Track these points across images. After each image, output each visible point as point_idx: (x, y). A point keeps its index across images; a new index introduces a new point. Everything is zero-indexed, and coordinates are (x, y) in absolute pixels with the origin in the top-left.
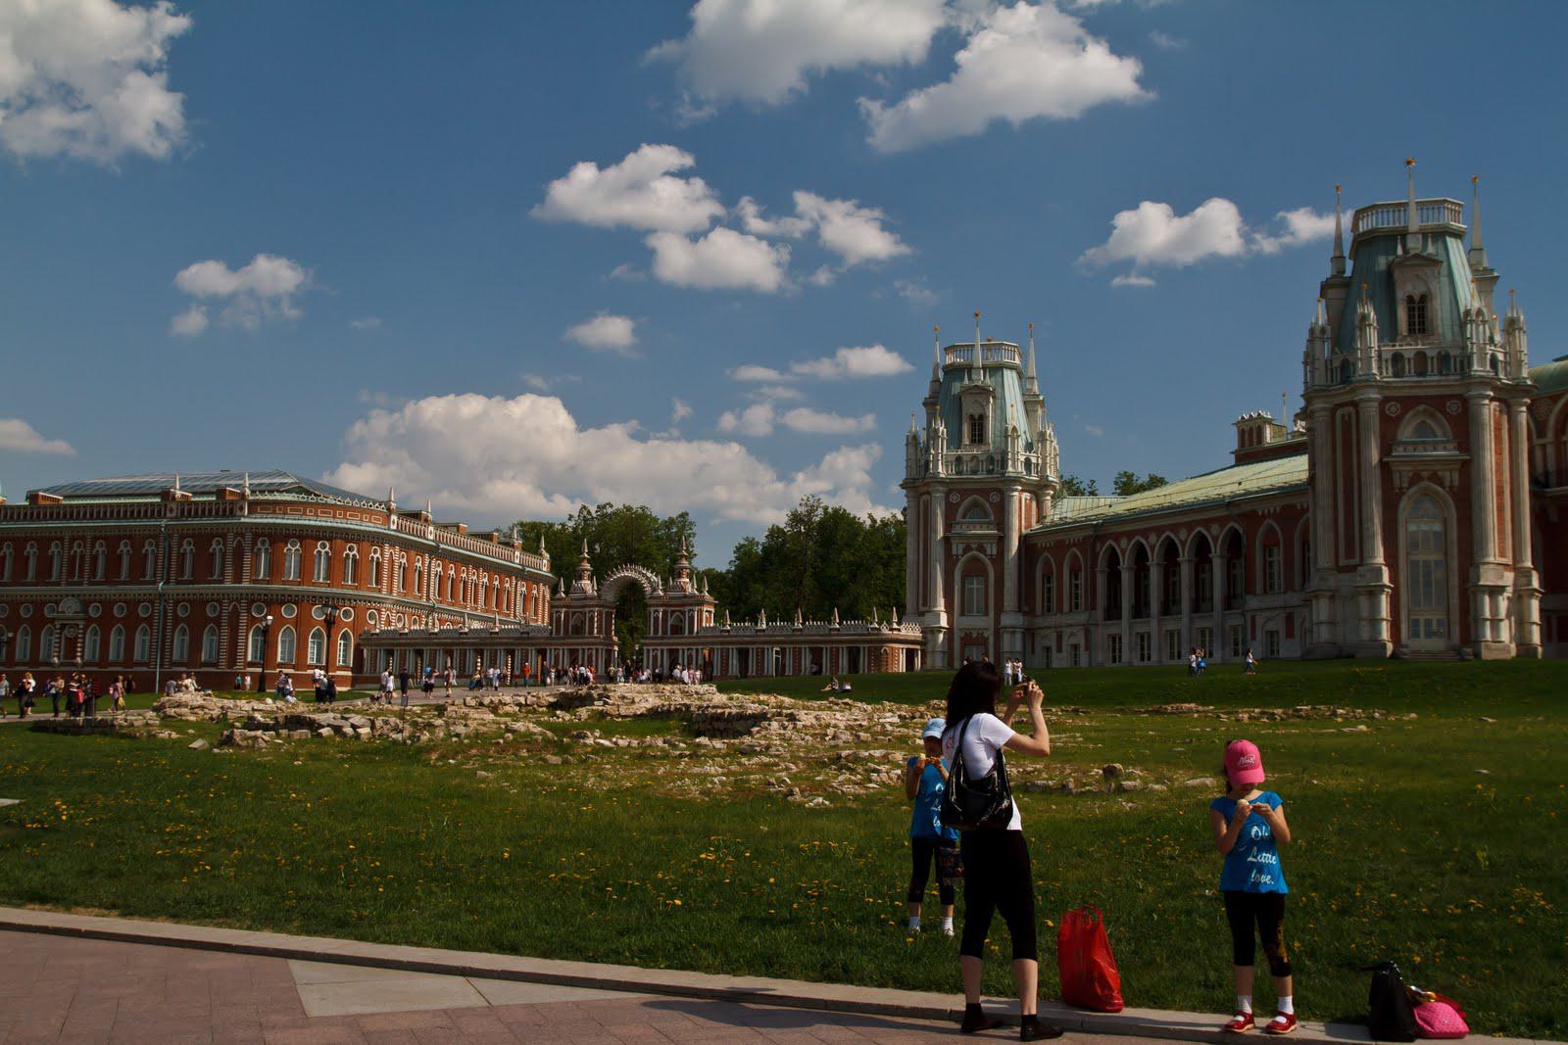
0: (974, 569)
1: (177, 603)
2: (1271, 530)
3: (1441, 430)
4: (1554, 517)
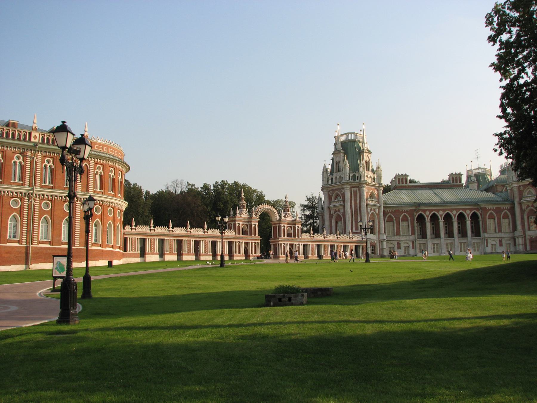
2: (491, 213)
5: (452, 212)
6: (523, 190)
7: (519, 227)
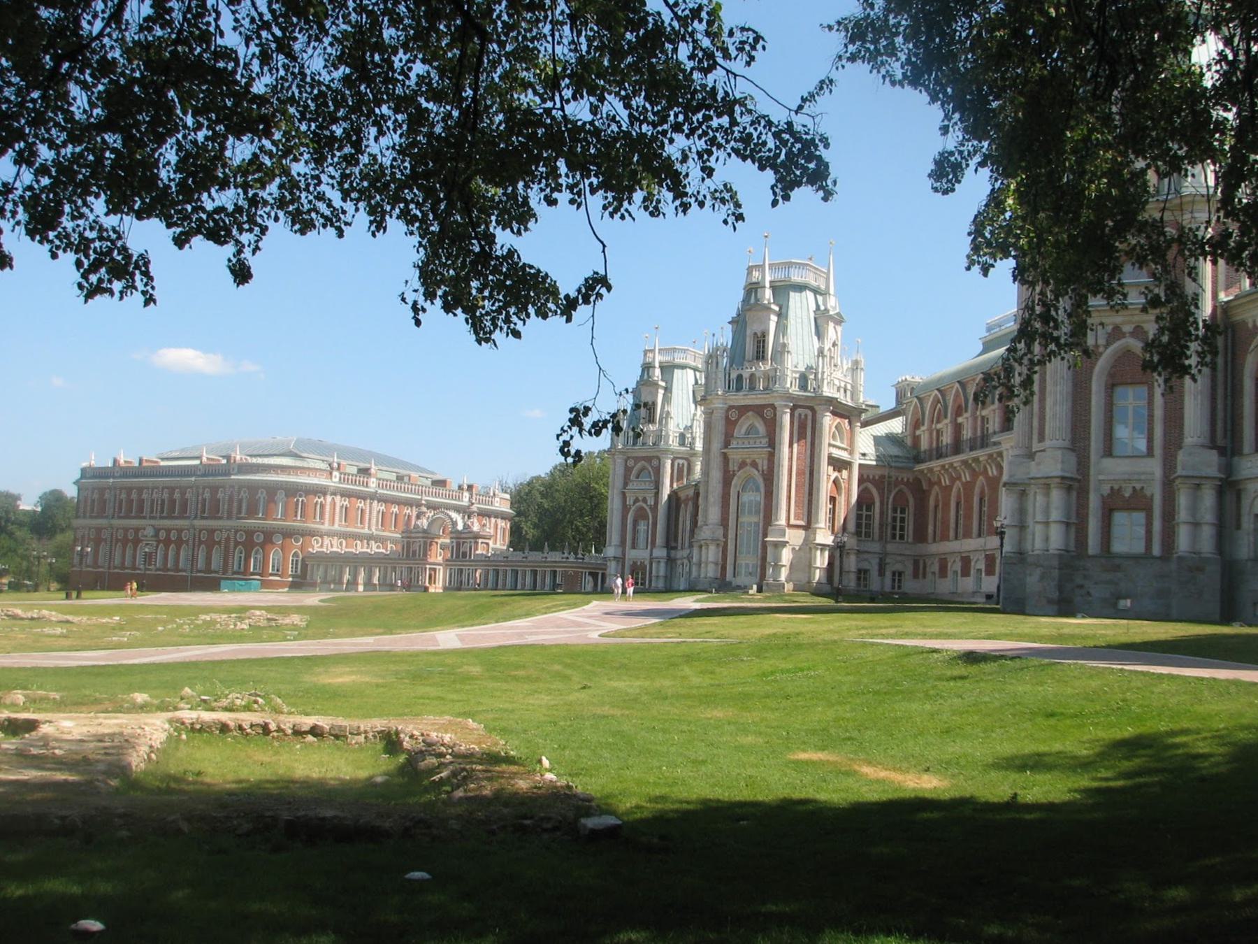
0: (641, 515)
1: (236, 532)
3: (761, 428)
4: (925, 487)
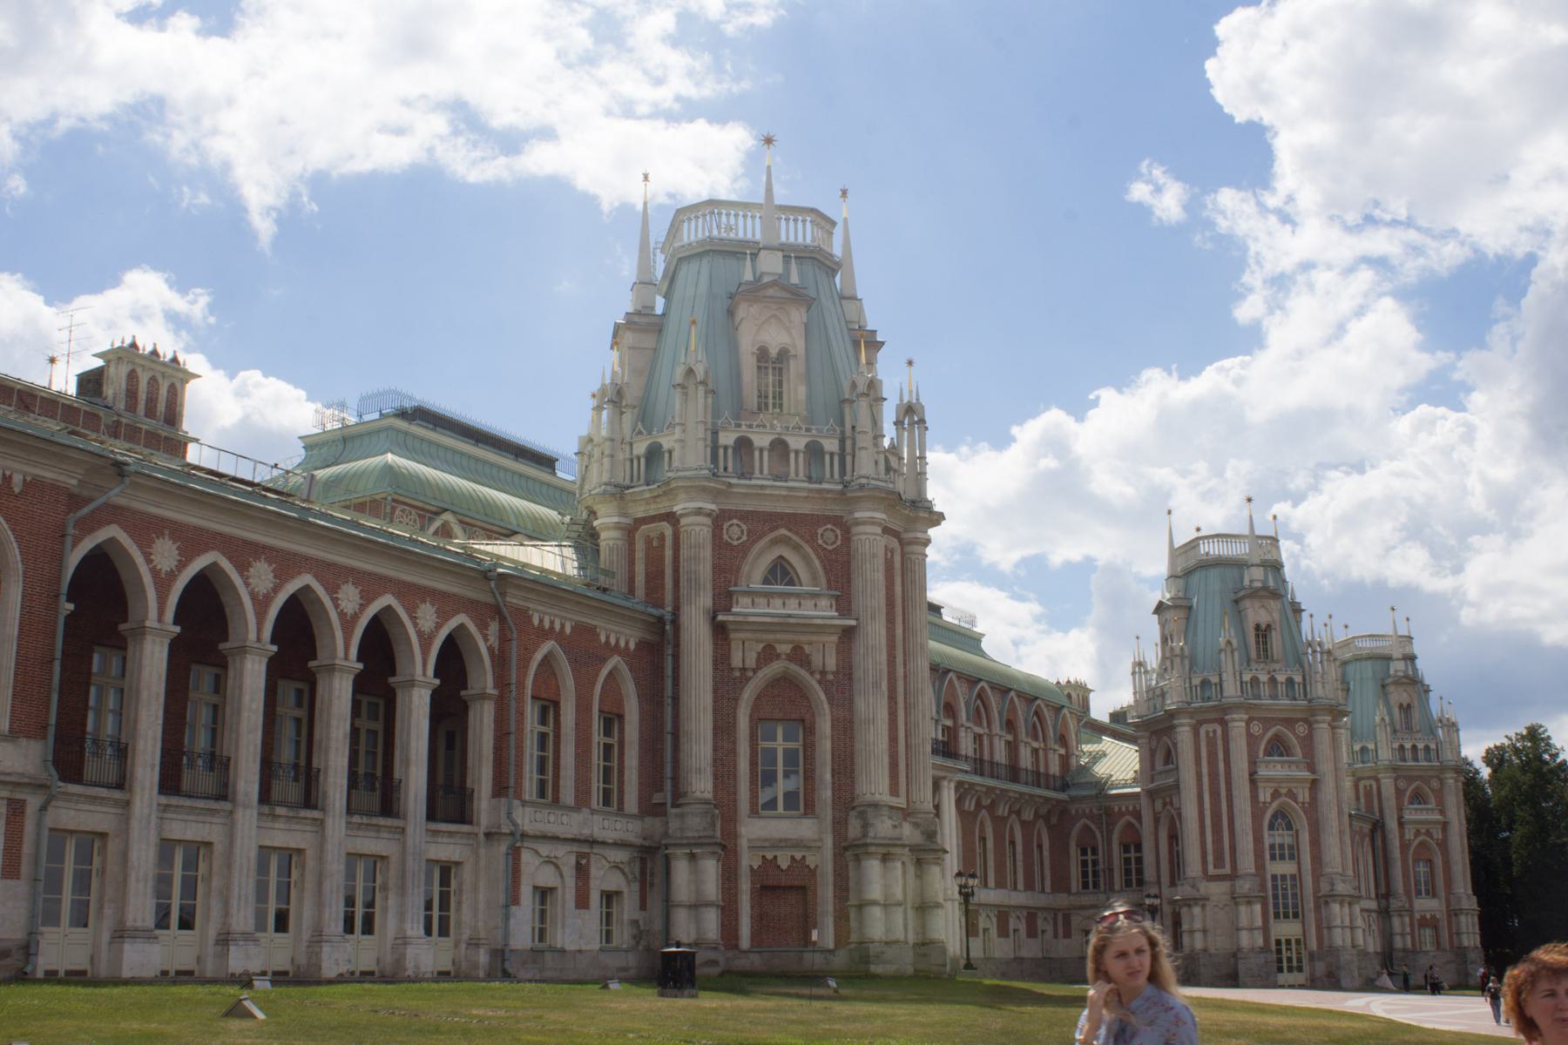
5: (332, 590)
6: (744, 550)
7: (701, 785)
